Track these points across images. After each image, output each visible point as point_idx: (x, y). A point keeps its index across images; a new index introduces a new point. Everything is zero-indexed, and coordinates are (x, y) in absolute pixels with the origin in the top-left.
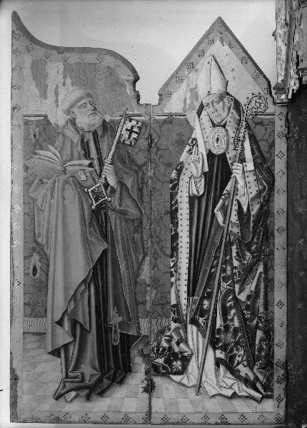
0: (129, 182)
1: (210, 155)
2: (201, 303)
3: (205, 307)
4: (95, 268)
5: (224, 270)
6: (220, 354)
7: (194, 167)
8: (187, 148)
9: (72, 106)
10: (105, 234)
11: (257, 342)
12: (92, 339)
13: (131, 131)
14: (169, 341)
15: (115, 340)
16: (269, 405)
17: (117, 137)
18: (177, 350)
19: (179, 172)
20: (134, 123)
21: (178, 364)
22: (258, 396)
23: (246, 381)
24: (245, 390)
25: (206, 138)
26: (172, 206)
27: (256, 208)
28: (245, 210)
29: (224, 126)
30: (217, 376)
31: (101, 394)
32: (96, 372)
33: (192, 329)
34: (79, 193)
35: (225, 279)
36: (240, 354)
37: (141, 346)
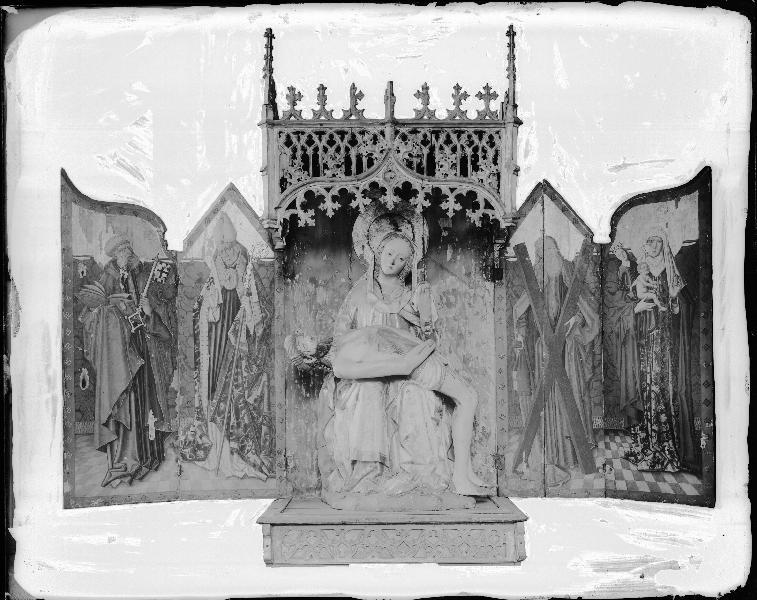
0: (161, 312)
1: (224, 291)
2: (218, 406)
3: (222, 408)
4: (134, 379)
5: (236, 380)
6: (234, 445)
7: (211, 302)
8: (206, 285)
9: (114, 250)
10: (144, 354)
11: (263, 434)
12: (133, 435)
13: (162, 271)
14: (194, 435)
15: (152, 435)
16: (272, 483)
17: (150, 277)
18: (200, 443)
19: (200, 304)
20: (164, 265)
21: (201, 453)
22: (264, 477)
23: (254, 466)
24: (253, 472)
25: (221, 279)
26: (194, 330)
27: (260, 332)
28: (252, 333)
29: (235, 268)
30: (232, 461)
31: (141, 479)
32: (135, 462)
33: (212, 426)
34: (121, 323)
35: (237, 386)
36: (249, 444)
37: (172, 440)
